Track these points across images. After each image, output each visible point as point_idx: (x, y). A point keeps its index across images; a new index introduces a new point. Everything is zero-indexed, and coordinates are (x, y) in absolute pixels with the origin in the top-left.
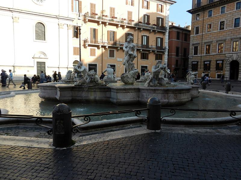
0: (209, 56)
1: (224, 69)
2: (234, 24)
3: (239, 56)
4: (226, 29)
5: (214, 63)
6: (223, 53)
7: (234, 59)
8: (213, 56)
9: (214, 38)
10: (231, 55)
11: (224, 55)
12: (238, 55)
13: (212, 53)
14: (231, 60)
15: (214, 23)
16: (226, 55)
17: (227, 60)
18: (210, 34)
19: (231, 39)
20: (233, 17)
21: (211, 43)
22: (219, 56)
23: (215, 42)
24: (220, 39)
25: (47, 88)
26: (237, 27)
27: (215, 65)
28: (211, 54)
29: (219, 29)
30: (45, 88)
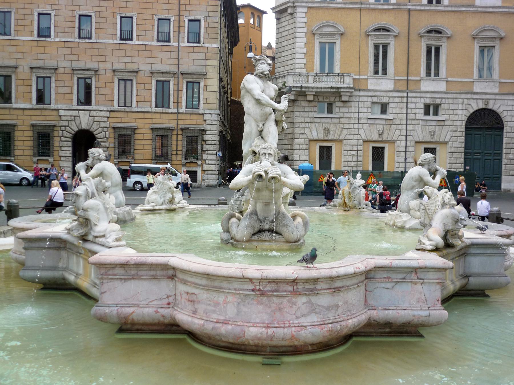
0: (7, 112)
1: (56, 153)
2: (77, 30)
3: (96, 119)
4: (55, 37)
5: (26, 133)
6: (53, 106)
7: (84, 126)
8: (20, 112)
9: (20, 56)
10: (75, 113)
11: (55, 113)
12: (94, 117)
13: (16, 103)
14: (76, 129)
15: (21, 11)
16: (62, 113)
17: (63, 128)
18: (8, 43)
19: (73, 70)
20: (72, 8)
21: (14, 70)
22: (38, 112)
23: (27, 69)
24: (40, 63)
25: (348, 283)
26: (87, 41)
27: (29, 138)
28: (15, 106)
29: (36, 33)
30: (337, 284)
